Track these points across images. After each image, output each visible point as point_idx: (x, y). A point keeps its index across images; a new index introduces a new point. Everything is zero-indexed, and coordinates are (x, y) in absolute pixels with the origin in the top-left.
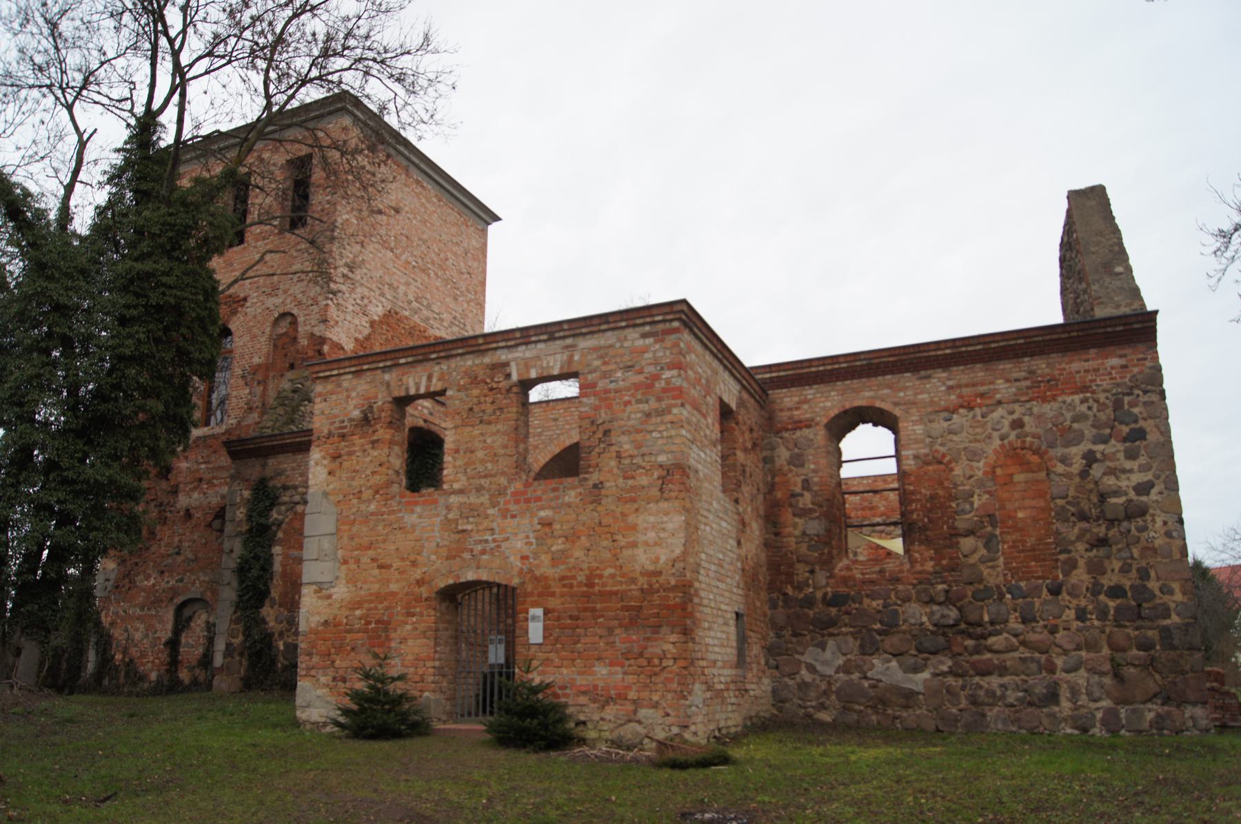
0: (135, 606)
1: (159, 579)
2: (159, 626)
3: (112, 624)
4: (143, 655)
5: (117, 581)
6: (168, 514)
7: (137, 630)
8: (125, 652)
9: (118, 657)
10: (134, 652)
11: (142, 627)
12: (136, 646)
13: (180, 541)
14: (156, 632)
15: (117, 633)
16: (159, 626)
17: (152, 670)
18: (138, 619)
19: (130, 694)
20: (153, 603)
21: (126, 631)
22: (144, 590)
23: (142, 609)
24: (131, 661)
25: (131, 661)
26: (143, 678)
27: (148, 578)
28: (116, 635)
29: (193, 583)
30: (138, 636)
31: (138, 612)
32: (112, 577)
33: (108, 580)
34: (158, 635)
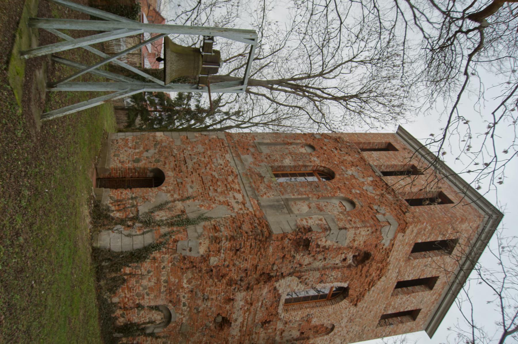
0: (168, 275)
1: (187, 290)
2: (152, 296)
3: (154, 258)
4: (130, 289)
5: (190, 257)
6: (233, 288)
7: (149, 280)
8: (131, 275)
9: (128, 270)
10: (133, 282)
11: (152, 284)
12: (137, 282)
13: (212, 299)
14: (148, 295)
15: (147, 265)
16: (152, 296)
17: (119, 297)
18: (158, 280)
19: (99, 288)
20: (170, 289)
21: (149, 272)
22: (179, 281)
23: (166, 281)
24: (124, 281)
25: (124, 281)
26: (112, 291)
27: (189, 282)
28: (145, 265)
29: (181, 314)
30: (145, 282)
31: (163, 278)
32: (193, 254)
33: (190, 250)
34: (146, 297)
